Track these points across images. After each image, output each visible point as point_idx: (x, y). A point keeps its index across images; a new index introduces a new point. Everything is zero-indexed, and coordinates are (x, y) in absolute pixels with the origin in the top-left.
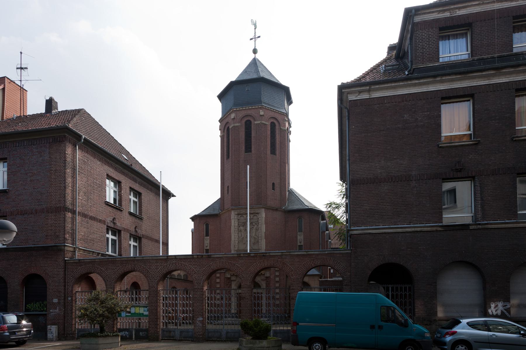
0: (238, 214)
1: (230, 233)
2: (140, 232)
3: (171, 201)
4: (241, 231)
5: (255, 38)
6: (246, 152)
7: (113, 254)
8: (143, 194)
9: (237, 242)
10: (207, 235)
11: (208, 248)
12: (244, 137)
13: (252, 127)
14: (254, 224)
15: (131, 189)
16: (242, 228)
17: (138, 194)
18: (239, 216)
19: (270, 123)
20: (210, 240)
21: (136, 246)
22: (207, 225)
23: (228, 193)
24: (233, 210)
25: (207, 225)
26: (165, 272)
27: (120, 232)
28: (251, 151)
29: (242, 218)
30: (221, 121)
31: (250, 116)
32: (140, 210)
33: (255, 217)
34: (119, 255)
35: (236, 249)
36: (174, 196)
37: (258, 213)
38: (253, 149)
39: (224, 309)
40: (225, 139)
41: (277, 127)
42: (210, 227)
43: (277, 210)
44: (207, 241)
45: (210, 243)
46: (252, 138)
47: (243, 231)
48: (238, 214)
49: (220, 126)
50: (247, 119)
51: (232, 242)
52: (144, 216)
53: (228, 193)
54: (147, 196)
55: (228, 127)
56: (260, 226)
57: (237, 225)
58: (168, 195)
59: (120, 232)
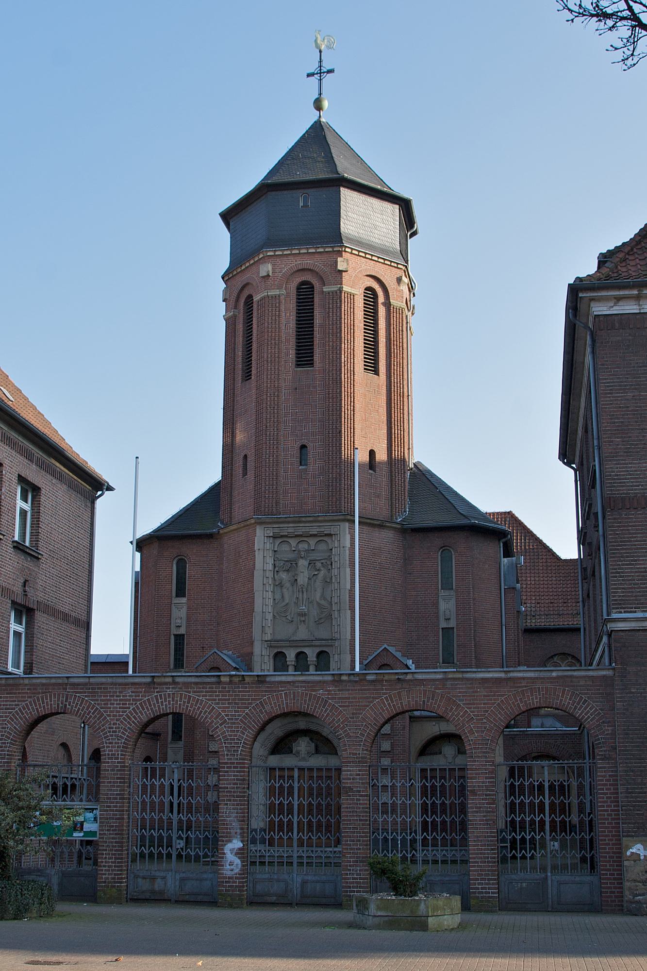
0: (274, 537)
1: (251, 591)
2: (36, 595)
3: (103, 503)
4: (281, 585)
5: (321, 73)
6: (298, 365)
7: (16, 671)
8: (43, 491)
9: (270, 617)
10: (181, 592)
11: (182, 631)
12: (292, 324)
13: (316, 300)
14: (318, 565)
15: (21, 479)
16: (284, 576)
17: (30, 489)
18: (278, 541)
19: (362, 290)
20: (189, 608)
21: (20, 634)
22: (182, 564)
23: (245, 473)
24: (261, 523)
25: (182, 564)
26: (145, 719)
27: (30, 611)
28: (311, 363)
29: (285, 547)
30: (227, 277)
31: (310, 270)
32: (35, 534)
33: (322, 547)
34: (25, 673)
35: (268, 637)
36: (110, 488)
37: (330, 535)
38: (317, 357)
39: (175, 817)
40: (240, 327)
41: (381, 299)
42: (190, 571)
43: (381, 526)
44: (180, 610)
45: (188, 619)
46: (316, 329)
47: (288, 585)
48: (274, 537)
49: (225, 291)
50: (304, 278)
51: (257, 619)
52: (43, 550)
53: (245, 473)
54: (55, 493)
55: (250, 297)
56: (335, 572)
57: (271, 567)
58: (93, 485)
59: (30, 611)
